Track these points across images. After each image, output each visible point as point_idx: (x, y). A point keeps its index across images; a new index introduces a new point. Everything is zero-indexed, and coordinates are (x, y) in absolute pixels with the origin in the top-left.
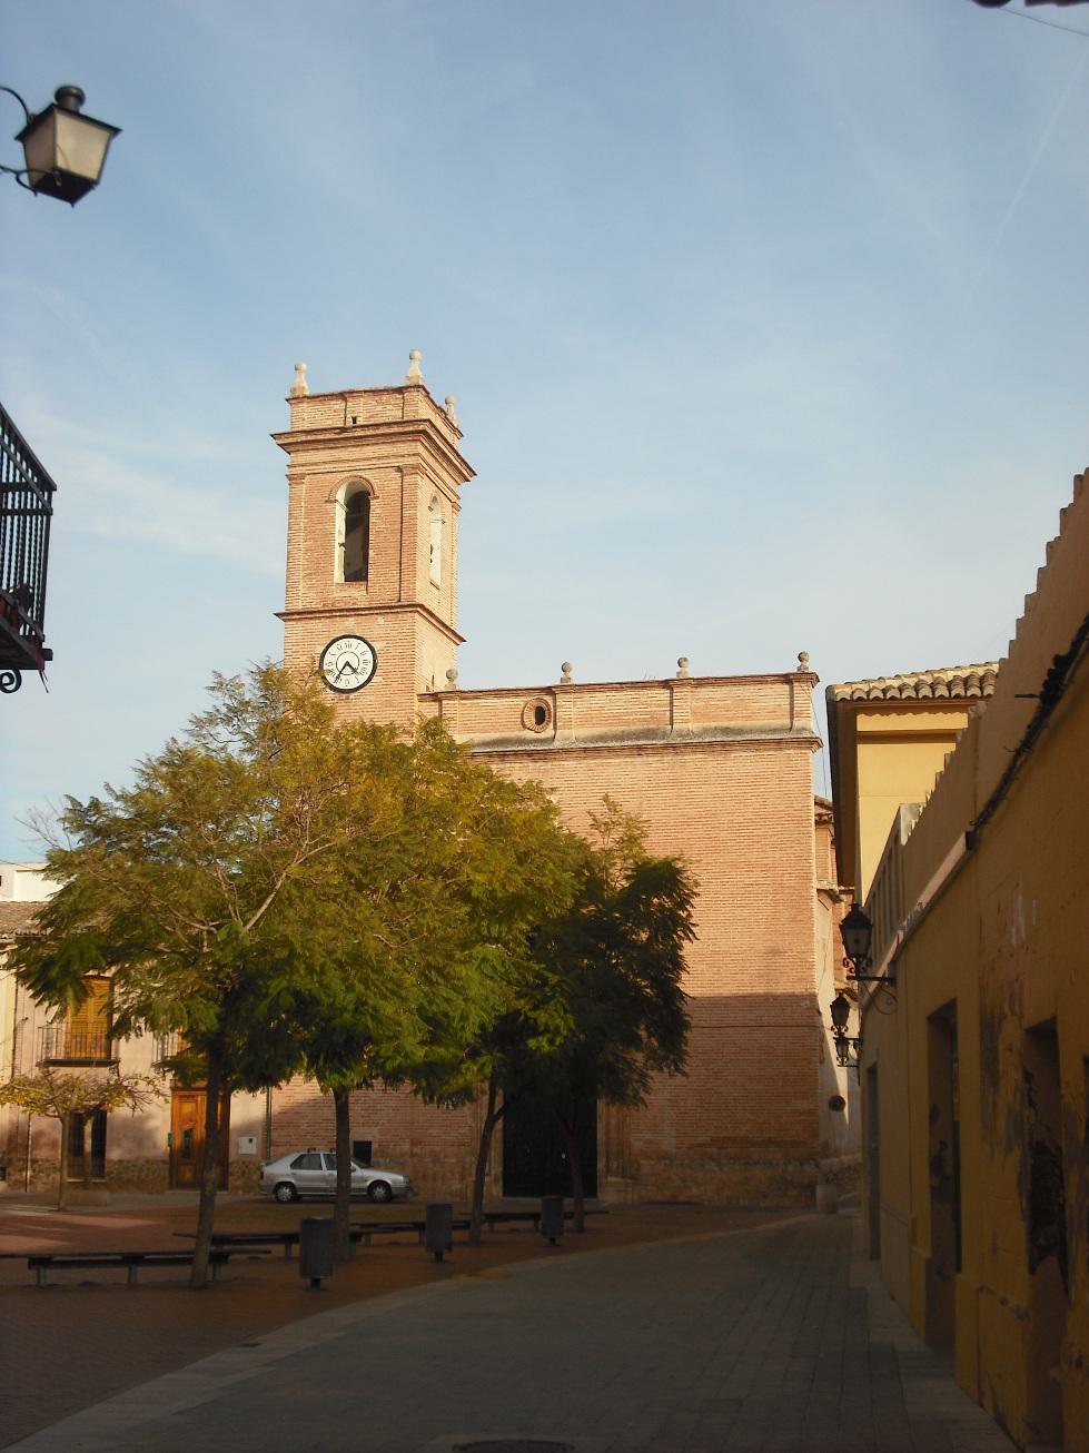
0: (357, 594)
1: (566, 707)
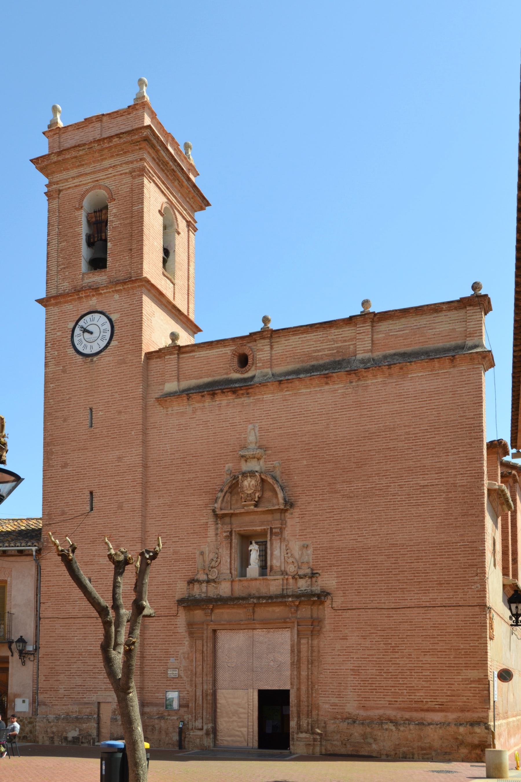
0: (99, 278)
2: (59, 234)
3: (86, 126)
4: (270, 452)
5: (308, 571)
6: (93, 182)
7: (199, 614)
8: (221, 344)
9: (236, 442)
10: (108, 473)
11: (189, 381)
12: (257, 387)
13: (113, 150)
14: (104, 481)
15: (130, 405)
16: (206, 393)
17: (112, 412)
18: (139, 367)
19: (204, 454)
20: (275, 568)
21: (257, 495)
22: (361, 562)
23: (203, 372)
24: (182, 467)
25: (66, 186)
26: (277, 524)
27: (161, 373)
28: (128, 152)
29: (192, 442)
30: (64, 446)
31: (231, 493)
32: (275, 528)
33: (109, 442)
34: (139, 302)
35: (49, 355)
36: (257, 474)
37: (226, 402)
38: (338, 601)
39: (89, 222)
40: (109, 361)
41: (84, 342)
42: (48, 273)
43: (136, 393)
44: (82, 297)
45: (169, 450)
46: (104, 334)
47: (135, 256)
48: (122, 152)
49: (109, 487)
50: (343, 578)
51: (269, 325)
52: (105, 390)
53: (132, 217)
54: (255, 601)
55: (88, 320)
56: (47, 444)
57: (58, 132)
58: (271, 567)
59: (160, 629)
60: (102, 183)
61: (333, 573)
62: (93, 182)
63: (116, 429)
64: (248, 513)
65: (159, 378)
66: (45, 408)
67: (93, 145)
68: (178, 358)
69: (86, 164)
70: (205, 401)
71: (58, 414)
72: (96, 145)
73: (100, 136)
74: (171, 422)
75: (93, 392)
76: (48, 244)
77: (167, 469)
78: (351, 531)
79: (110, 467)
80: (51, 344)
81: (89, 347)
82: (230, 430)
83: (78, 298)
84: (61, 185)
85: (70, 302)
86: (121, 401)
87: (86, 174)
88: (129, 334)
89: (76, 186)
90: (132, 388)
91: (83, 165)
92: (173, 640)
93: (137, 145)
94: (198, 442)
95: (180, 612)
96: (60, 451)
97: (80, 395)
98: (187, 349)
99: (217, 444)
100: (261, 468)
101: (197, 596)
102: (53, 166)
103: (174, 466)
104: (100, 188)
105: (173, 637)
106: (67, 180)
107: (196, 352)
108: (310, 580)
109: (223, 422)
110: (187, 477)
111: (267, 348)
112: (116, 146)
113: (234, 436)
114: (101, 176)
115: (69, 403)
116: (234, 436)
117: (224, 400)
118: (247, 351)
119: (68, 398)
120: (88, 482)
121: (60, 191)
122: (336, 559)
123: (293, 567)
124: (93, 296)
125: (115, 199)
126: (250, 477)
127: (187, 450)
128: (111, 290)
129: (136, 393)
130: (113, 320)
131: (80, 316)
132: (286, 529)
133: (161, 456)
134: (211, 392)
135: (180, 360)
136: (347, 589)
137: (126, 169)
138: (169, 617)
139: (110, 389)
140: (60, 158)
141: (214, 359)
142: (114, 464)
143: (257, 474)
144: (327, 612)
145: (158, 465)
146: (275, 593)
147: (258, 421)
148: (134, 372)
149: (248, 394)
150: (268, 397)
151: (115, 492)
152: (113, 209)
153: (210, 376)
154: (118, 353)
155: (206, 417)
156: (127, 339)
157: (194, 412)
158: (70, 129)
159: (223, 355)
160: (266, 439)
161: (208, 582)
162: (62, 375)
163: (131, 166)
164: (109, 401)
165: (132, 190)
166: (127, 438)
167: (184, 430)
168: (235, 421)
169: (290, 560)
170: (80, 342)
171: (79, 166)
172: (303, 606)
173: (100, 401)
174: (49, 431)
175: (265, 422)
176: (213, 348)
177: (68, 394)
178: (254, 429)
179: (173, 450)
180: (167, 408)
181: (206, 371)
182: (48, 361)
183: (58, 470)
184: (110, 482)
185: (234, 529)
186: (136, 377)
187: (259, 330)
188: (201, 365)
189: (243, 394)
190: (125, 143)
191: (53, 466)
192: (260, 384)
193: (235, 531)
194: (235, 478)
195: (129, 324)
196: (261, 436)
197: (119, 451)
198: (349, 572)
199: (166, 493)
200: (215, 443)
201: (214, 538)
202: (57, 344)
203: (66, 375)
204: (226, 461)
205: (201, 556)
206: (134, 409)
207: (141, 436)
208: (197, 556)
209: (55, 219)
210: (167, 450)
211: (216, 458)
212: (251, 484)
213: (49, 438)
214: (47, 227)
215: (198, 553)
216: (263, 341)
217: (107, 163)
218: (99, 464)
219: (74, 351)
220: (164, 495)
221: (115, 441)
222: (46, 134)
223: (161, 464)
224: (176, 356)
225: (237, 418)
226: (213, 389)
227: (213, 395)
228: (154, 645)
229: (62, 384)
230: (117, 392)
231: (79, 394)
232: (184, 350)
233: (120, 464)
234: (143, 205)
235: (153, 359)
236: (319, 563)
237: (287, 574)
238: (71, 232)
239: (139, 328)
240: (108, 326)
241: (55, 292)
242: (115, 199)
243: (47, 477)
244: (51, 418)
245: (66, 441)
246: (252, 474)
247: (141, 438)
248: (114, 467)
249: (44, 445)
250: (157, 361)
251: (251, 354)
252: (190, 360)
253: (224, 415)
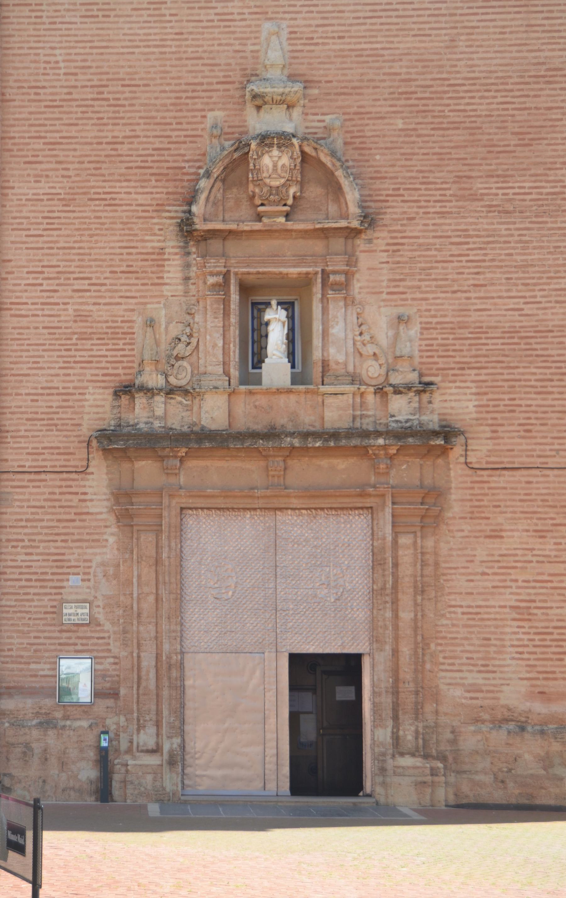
4: (316, 91)
5: (413, 377)
7: (146, 471)
20: (333, 365)
22: (530, 362)
26: (337, 264)
31: (224, 181)
32: (335, 272)
38: (480, 449)
50: (490, 396)
54: (296, 442)
58: (325, 364)
59: (43, 503)
61: (468, 384)
64: (269, 233)
78: (508, 291)
92: (76, 531)
95: (92, 463)
101: (142, 426)
105: (77, 523)
108: (417, 399)
122: (474, 353)
123: (377, 367)
127: (109, 67)
132: (357, 276)
136: (500, 422)
138: (65, 476)
143: (295, 141)
144: (454, 473)
146: (337, 425)
147: (286, 16)
161: (170, 391)
169: (370, 349)
172: (398, 457)
185: (233, 270)
193: (236, 274)
194: (242, 146)
196: (293, 51)
198: (506, 384)
201: (180, 287)
205: (149, 330)
208: (138, 327)
215: (139, 321)
228: (27, 543)
236: (436, 359)
237: (362, 383)
246: (283, 140)
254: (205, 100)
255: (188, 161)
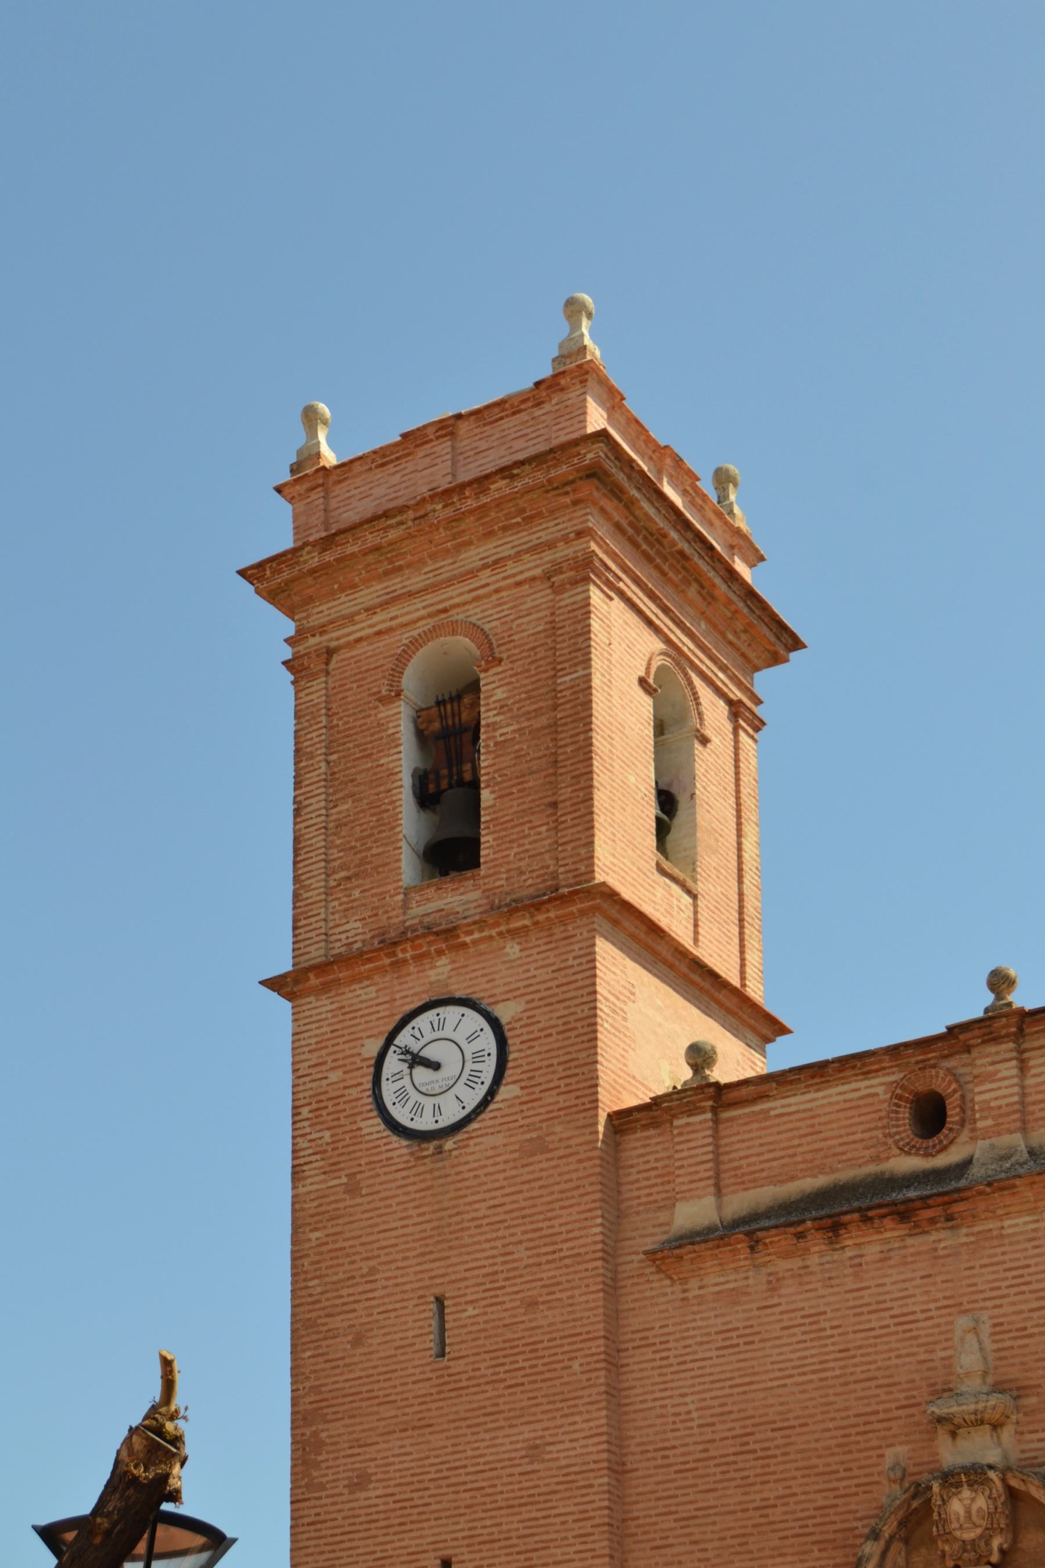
0: (458, 898)
1: (993, 1083)
2: (331, 778)
3: (408, 455)
4: (1033, 1400)
6: (430, 615)
8: (854, 1067)
9: (915, 1376)
10: (499, 1497)
11: (752, 1192)
12: (981, 1193)
13: (493, 514)
14: (488, 1523)
15: (564, 1279)
16: (809, 1224)
17: (508, 1305)
18: (590, 1159)
19: (809, 1421)
21: (996, 1543)
23: (799, 1158)
24: (740, 1465)
25: (349, 634)
27: (660, 1172)
28: (540, 515)
29: (770, 1384)
30: (358, 1420)
31: (906, 1541)
33: (500, 1401)
34: (584, 960)
35: (306, 1145)
36: (992, 1474)
37: (877, 1248)
39: (421, 735)
40: (494, 1148)
41: (415, 1096)
42: (296, 897)
43: (582, 1241)
44: (405, 961)
45: (695, 1415)
46: (477, 1067)
47: (569, 823)
48: (519, 519)
49: (503, 1543)
51: (1010, 998)
52: (482, 1238)
53: (555, 707)
55: (426, 1029)
56: (300, 1419)
57: (320, 481)
60: (461, 617)
62: (430, 615)
63: (520, 1358)
65: (656, 1189)
66: (293, 1307)
67: (429, 507)
68: (716, 1121)
69: (409, 565)
70: (807, 1249)
71: (336, 1323)
72: (440, 506)
73: (449, 478)
74: (699, 1323)
75: (444, 1246)
76: (297, 813)
77: (689, 1474)
79: (505, 1480)
80: (309, 1109)
81: (428, 1111)
82: (893, 1338)
83: (392, 964)
84: (334, 635)
85: (368, 978)
86: (534, 1269)
87: (410, 594)
88: (555, 1061)
89: (379, 633)
90: (569, 1227)
91: (400, 568)
93: (567, 493)
94: (788, 1381)
96: (345, 1438)
97: (405, 1259)
98: (744, 1091)
99: (853, 1387)
100: (1005, 1457)
102: (309, 580)
103: (712, 1463)
104: (454, 633)
106: (350, 619)
107: (774, 1098)
109: (870, 1312)
110: (758, 1497)
111: (1009, 1069)
112: (499, 504)
113: (908, 1355)
114: (455, 594)
115: (369, 1287)
116: (908, 1355)
117: (870, 1245)
118: (940, 1083)
119: (365, 1270)
120: (436, 1530)
121: (330, 652)
124: (440, 953)
125: (501, 660)
126: (970, 1485)
127: (755, 1408)
128: (494, 932)
129: (582, 1241)
130: (504, 1020)
131: (398, 1017)
133: (670, 1435)
134: (829, 1221)
135: (721, 1126)
137: (533, 566)
139: (500, 1234)
140: (329, 557)
141: (833, 1117)
142: (519, 1469)
145: (660, 1462)
147: (988, 1304)
148: (574, 1176)
149: (949, 1218)
150: (1018, 1224)
151: (522, 1557)
152: (495, 690)
153: (821, 1169)
154: (522, 1122)
155: (812, 1303)
156: (550, 1077)
157: (774, 1285)
158: (357, 468)
159: (861, 1102)
160: (1017, 1360)
162: (348, 1203)
163: (548, 556)
164: (496, 1273)
165: (553, 628)
166: (557, 1382)
167: (742, 1348)
168: (911, 1309)
170: (402, 1095)
171: (386, 573)
173: (467, 1274)
174: (308, 1378)
175: (1013, 1304)
176: (827, 1083)
177: (368, 1259)
178: (975, 1330)
179: (708, 1412)
180: (684, 1281)
181: (809, 1156)
182: (302, 1161)
183: (339, 1499)
184: (504, 1527)
186: (582, 1191)
187: (979, 1014)
188: (790, 1139)
189: (932, 1221)
190: (529, 490)
191: (322, 1487)
192: (989, 1184)
194: (920, 1490)
195: (553, 1031)
196: (999, 1350)
197: (532, 1427)
199: (692, 1552)
200: (847, 1384)
202: (331, 1109)
203: (359, 1200)
204: (885, 1438)
206: (577, 1292)
207: (603, 1373)
209: (316, 737)
210: (689, 1412)
211: (853, 1431)
212: (974, 1508)
213: (308, 1400)
214: (292, 761)
216: (993, 1049)
217: (471, 557)
218: (471, 1469)
219: (383, 1127)
220: (683, 1558)
221: (519, 1396)
222: (286, 491)
223: (672, 1460)
224: (709, 1116)
225: (919, 1298)
226: (831, 1212)
227: (834, 1228)
229: (346, 1228)
230: (520, 1242)
231: (400, 1256)
232: (734, 1095)
233: (535, 1466)
234: (590, 667)
235: (634, 1131)
238: (368, 770)
239: (585, 1038)
240: (488, 1041)
241: (322, 952)
242: (501, 660)
243: (306, 1520)
244: (314, 1337)
245: (364, 1404)
247: (602, 1380)
248: (517, 1478)
249: (293, 1421)
250: (648, 1138)
251: (955, 1091)
252: (755, 1126)
253: (874, 1290)
254: (883, 1433)
255: (860, 1519)
